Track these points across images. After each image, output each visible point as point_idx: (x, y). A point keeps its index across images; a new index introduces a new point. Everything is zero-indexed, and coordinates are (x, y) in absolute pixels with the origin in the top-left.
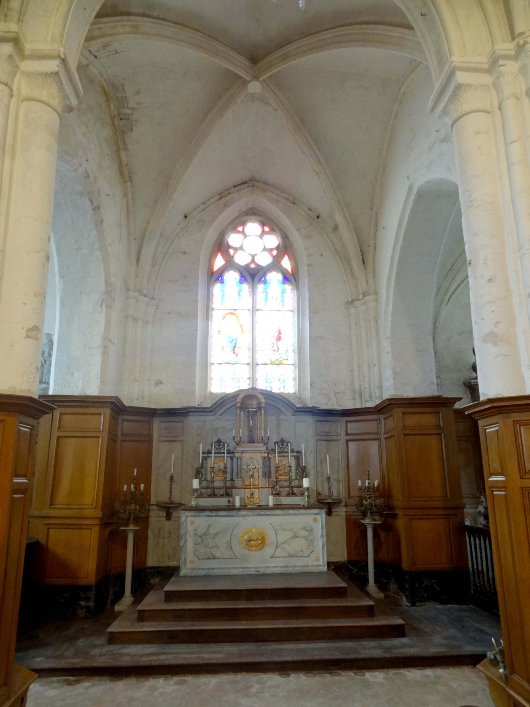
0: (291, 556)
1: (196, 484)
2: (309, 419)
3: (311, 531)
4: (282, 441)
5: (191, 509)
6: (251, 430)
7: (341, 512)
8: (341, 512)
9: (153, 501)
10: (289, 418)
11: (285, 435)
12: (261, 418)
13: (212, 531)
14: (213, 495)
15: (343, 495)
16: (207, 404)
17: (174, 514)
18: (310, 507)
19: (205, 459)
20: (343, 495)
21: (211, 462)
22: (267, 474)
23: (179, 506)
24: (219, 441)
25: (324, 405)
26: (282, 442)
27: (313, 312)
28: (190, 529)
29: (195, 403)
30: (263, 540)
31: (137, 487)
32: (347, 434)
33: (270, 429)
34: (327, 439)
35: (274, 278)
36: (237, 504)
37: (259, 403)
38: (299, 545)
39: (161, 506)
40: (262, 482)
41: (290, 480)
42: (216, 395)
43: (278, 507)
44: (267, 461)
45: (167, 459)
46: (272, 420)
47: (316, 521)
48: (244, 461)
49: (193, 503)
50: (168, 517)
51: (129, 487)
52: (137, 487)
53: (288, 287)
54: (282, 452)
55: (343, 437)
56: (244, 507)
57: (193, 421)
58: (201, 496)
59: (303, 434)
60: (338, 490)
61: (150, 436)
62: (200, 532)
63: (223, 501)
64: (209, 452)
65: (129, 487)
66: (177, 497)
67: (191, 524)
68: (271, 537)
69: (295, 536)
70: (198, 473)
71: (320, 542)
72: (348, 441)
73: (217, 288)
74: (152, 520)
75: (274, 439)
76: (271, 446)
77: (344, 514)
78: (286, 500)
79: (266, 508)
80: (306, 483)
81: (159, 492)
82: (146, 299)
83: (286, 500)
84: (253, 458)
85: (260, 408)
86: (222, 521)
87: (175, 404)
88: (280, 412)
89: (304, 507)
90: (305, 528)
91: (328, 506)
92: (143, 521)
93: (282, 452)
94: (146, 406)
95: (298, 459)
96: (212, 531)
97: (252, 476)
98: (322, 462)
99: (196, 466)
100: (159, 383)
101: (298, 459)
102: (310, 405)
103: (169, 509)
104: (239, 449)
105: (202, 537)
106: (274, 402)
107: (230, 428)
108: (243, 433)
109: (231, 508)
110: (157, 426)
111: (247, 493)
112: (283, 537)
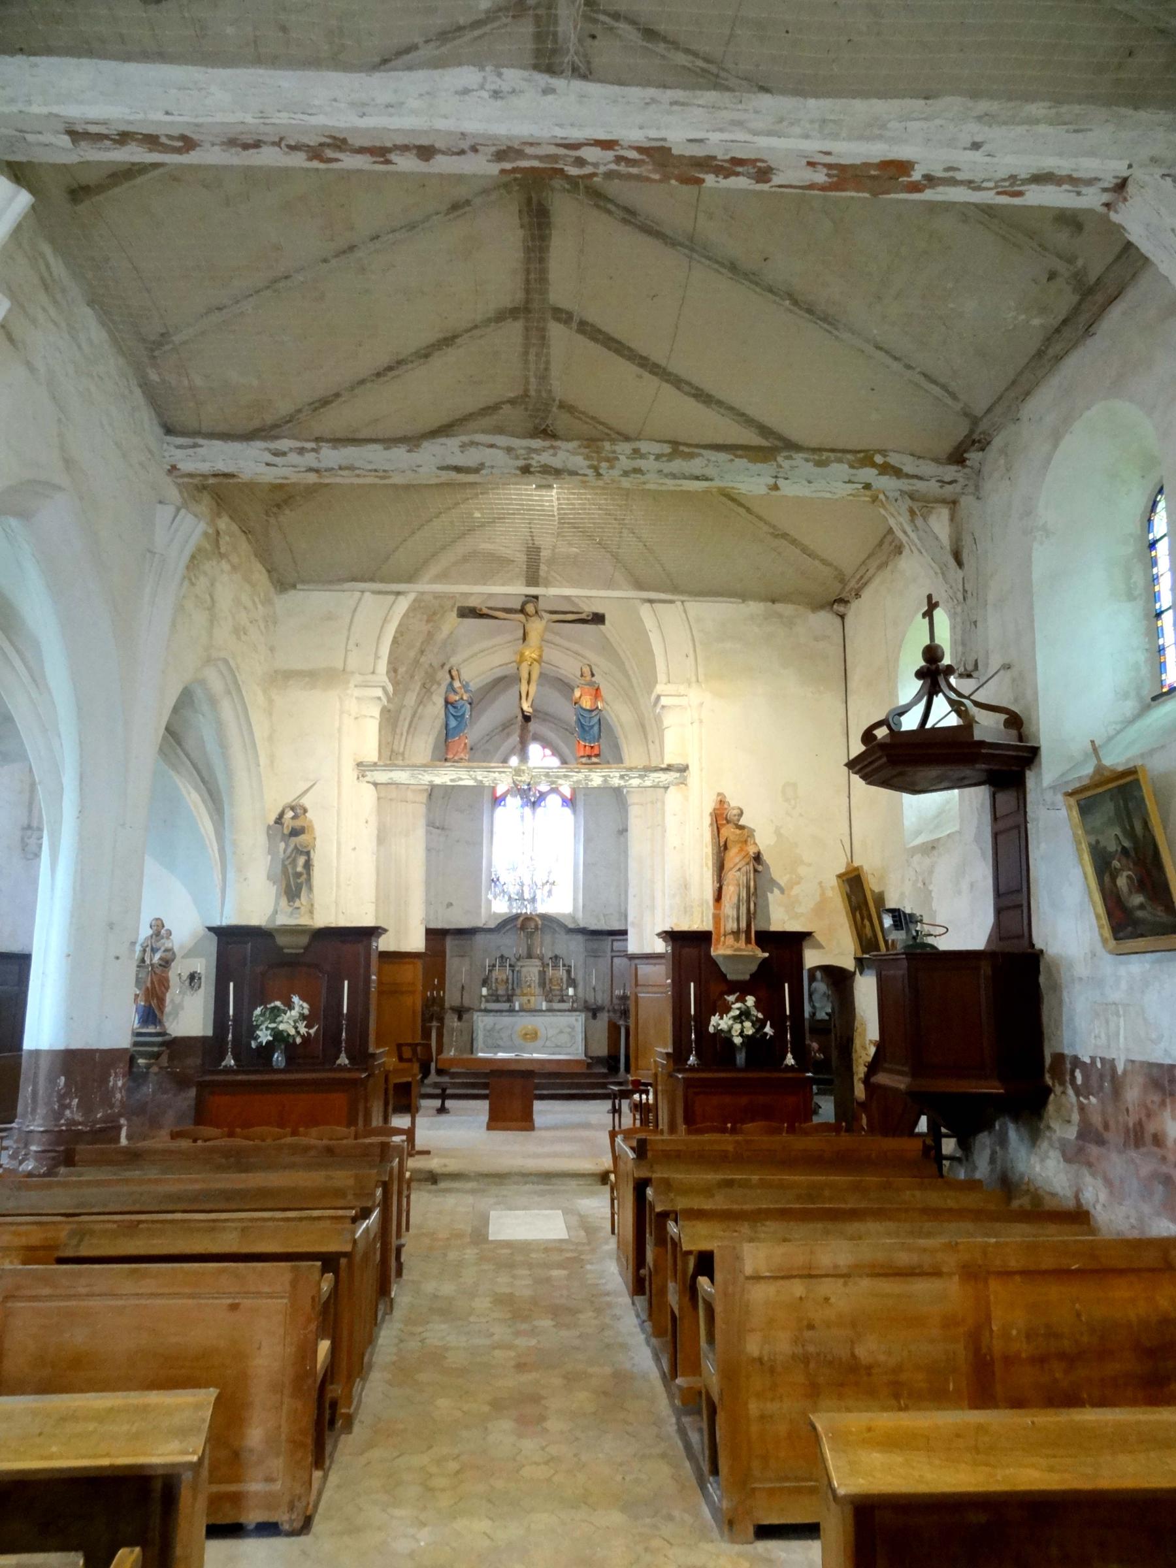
0: (557, 1046)
1: (484, 991)
2: (580, 938)
3: (573, 1028)
4: (556, 957)
5: (481, 1010)
6: (529, 948)
7: (604, 1018)
8: (604, 1018)
9: (447, 1005)
10: (562, 937)
11: (558, 952)
12: (538, 937)
13: (498, 1027)
14: (497, 1001)
15: (607, 1003)
16: (492, 925)
17: (465, 1016)
18: (572, 1010)
19: (490, 971)
20: (607, 1003)
21: (496, 973)
22: (542, 984)
23: (468, 1010)
24: (502, 957)
25: (594, 925)
26: (556, 958)
27: (588, 840)
28: (481, 1025)
29: (480, 923)
30: (536, 1033)
31: (438, 993)
32: (612, 950)
33: (545, 946)
34: (594, 954)
35: (553, 801)
36: (517, 1008)
37: (536, 926)
38: (564, 1038)
39: (453, 1009)
40: (538, 991)
41: (561, 990)
42: (500, 915)
43: (549, 1010)
44: (542, 974)
45: (458, 969)
46: (548, 938)
47: (577, 1021)
48: (523, 974)
49: (483, 1007)
50: (460, 1018)
51: (432, 994)
52: (438, 993)
53: (567, 811)
54: (555, 967)
55: (609, 954)
56: (522, 1010)
57: (479, 939)
58: (487, 1001)
59: (573, 950)
60: (602, 998)
61: (444, 952)
62: (488, 1027)
63: (506, 1006)
64: (494, 966)
65: (432, 994)
66: (466, 1003)
67: (482, 1022)
68: (542, 1032)
69: (561, 1032)
70: (485, 982)
71: (580, 1037)
72: (612, 957)
73: (499, 811)
74: (447, 1021)
75: (550, 955)
76: (547, 960)
77: (606, 1019)
78: (556, 1006)
79: (541, 1011)
80: (571, 991)
81: (452, 997)
82: (439, 831)
83: (556, 1006)
84: (531, 971)
85: (536, 928)
86: (506, 1020)
87: (464, 924)
88: (554, 932)
89: (569, 1011)
90: (569, 1026)
91: (593, 1011)
92: (441, 1020)
93: (555, 967)
94: (439, 927)
95: (569, 972)
96: (498, 1027)
97: (530, 986)
98: (590, 974)
99: (483, 977)
100: (450, 905)
101: (569, 972)
102: (582, 925)
103: (460, 1012)
104: (519, 964)
105: (490, 1031)
106: (549, 923)
107: (511, 945)
108: (522, 951)
109: (511, 1010)
110: (449, 943)
111: (525, 999)
112: (551, 1032)
